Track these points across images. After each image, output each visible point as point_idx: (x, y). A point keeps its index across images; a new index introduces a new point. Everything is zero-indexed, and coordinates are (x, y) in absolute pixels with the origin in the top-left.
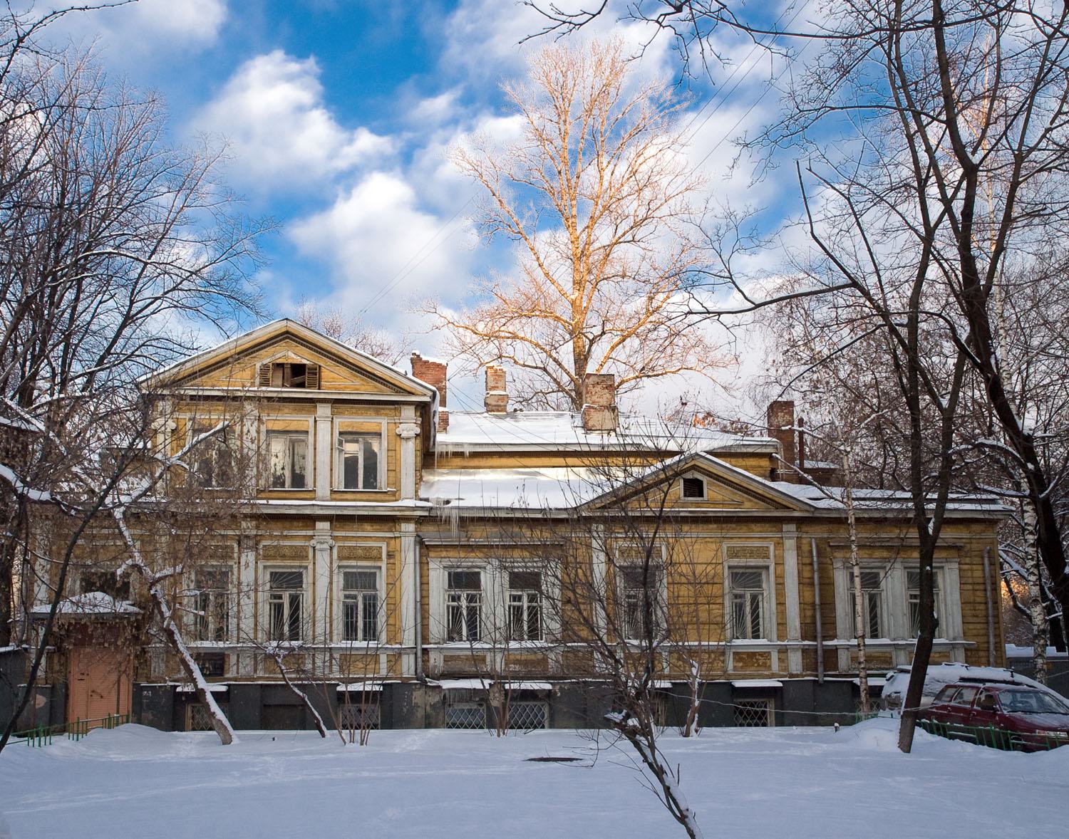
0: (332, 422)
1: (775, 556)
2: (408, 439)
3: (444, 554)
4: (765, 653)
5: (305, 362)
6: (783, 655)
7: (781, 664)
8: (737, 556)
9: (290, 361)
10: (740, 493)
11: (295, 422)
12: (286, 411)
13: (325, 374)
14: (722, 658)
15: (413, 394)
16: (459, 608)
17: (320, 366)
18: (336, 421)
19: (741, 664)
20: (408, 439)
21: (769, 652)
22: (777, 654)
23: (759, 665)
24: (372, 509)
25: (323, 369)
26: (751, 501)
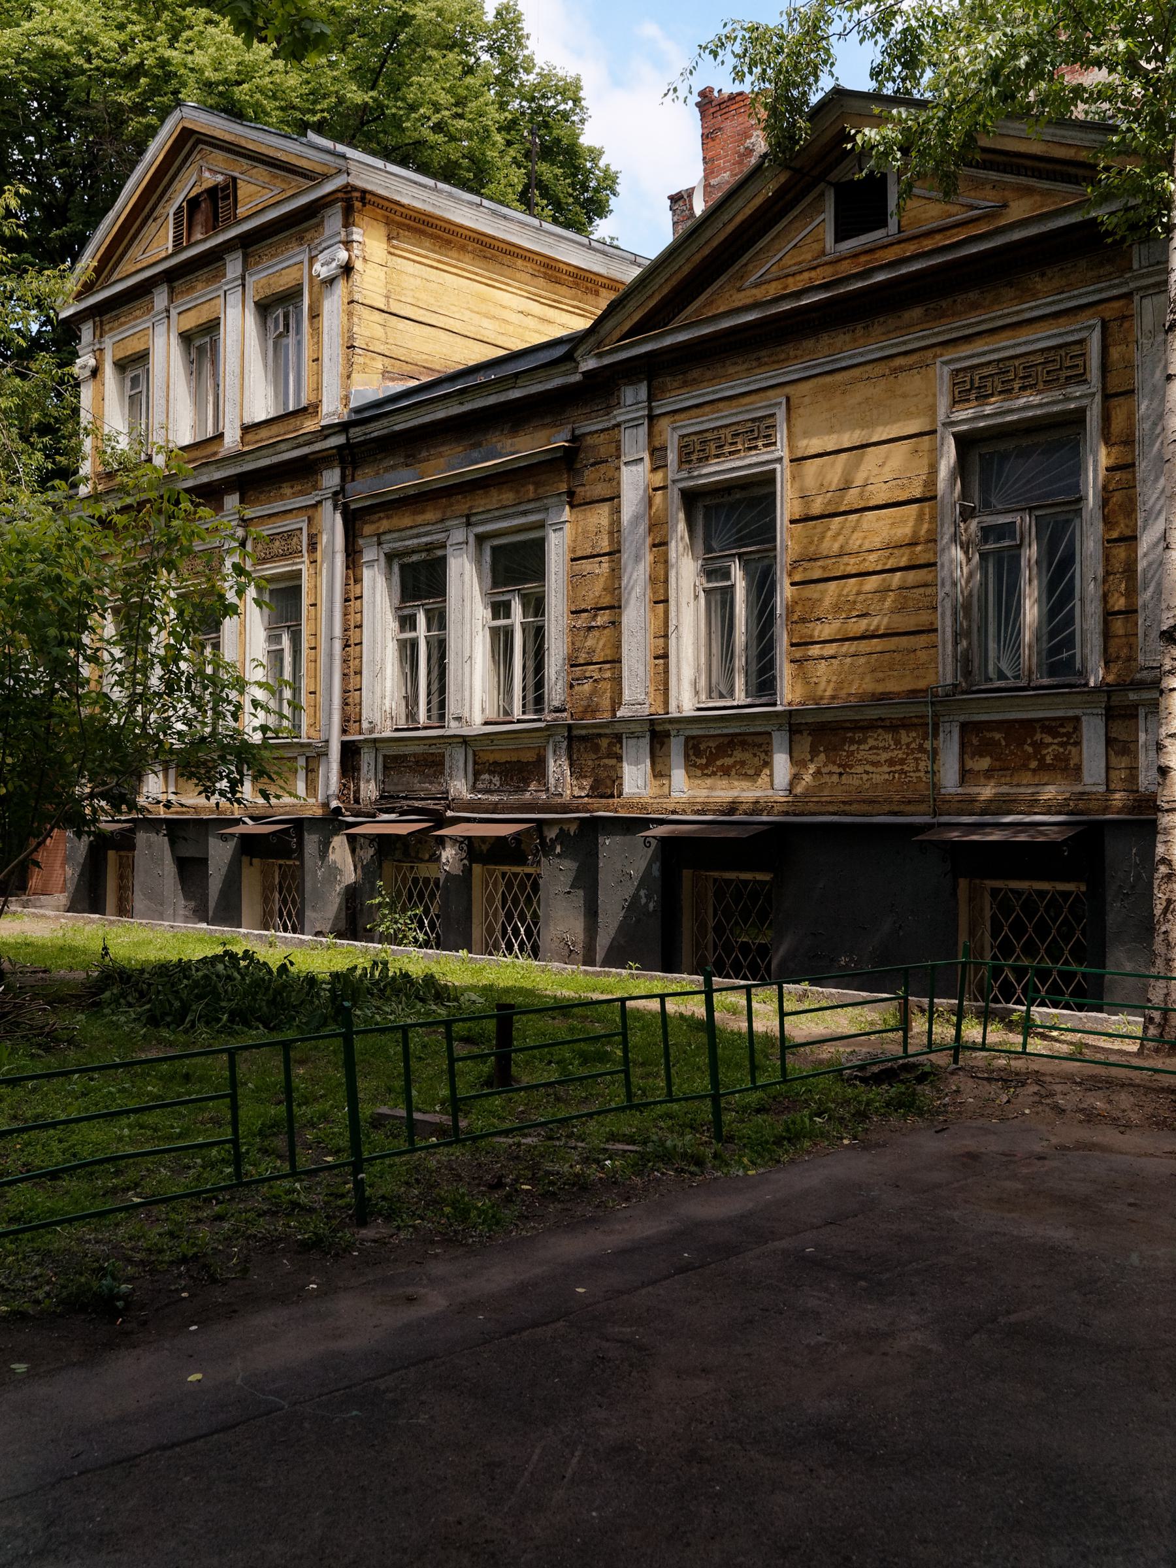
0: (244, 285)
1: (1105, 368)
2: (330, 281)
3: (385, 525)
4: (1063, 721)
5: (220, 178)
6: (1119, 732)
7: (1114, 761)
8: (983, 398)
9: (205, 186)
10: (993, 175)
11: (206, 306)
12: (200, 286)
13: (244, 190)
14: (928, 745)
15: (326, 177)
16: (414, 644)
17: (234, 179)
18: (250, 280)
19: (985, 763)
20: (330, 281)
21: (1077, 719)
22: (1100, 723)
23: (1043, 767)
24: (271, 451)
25: (240, 183)
26: (1029, 191)
